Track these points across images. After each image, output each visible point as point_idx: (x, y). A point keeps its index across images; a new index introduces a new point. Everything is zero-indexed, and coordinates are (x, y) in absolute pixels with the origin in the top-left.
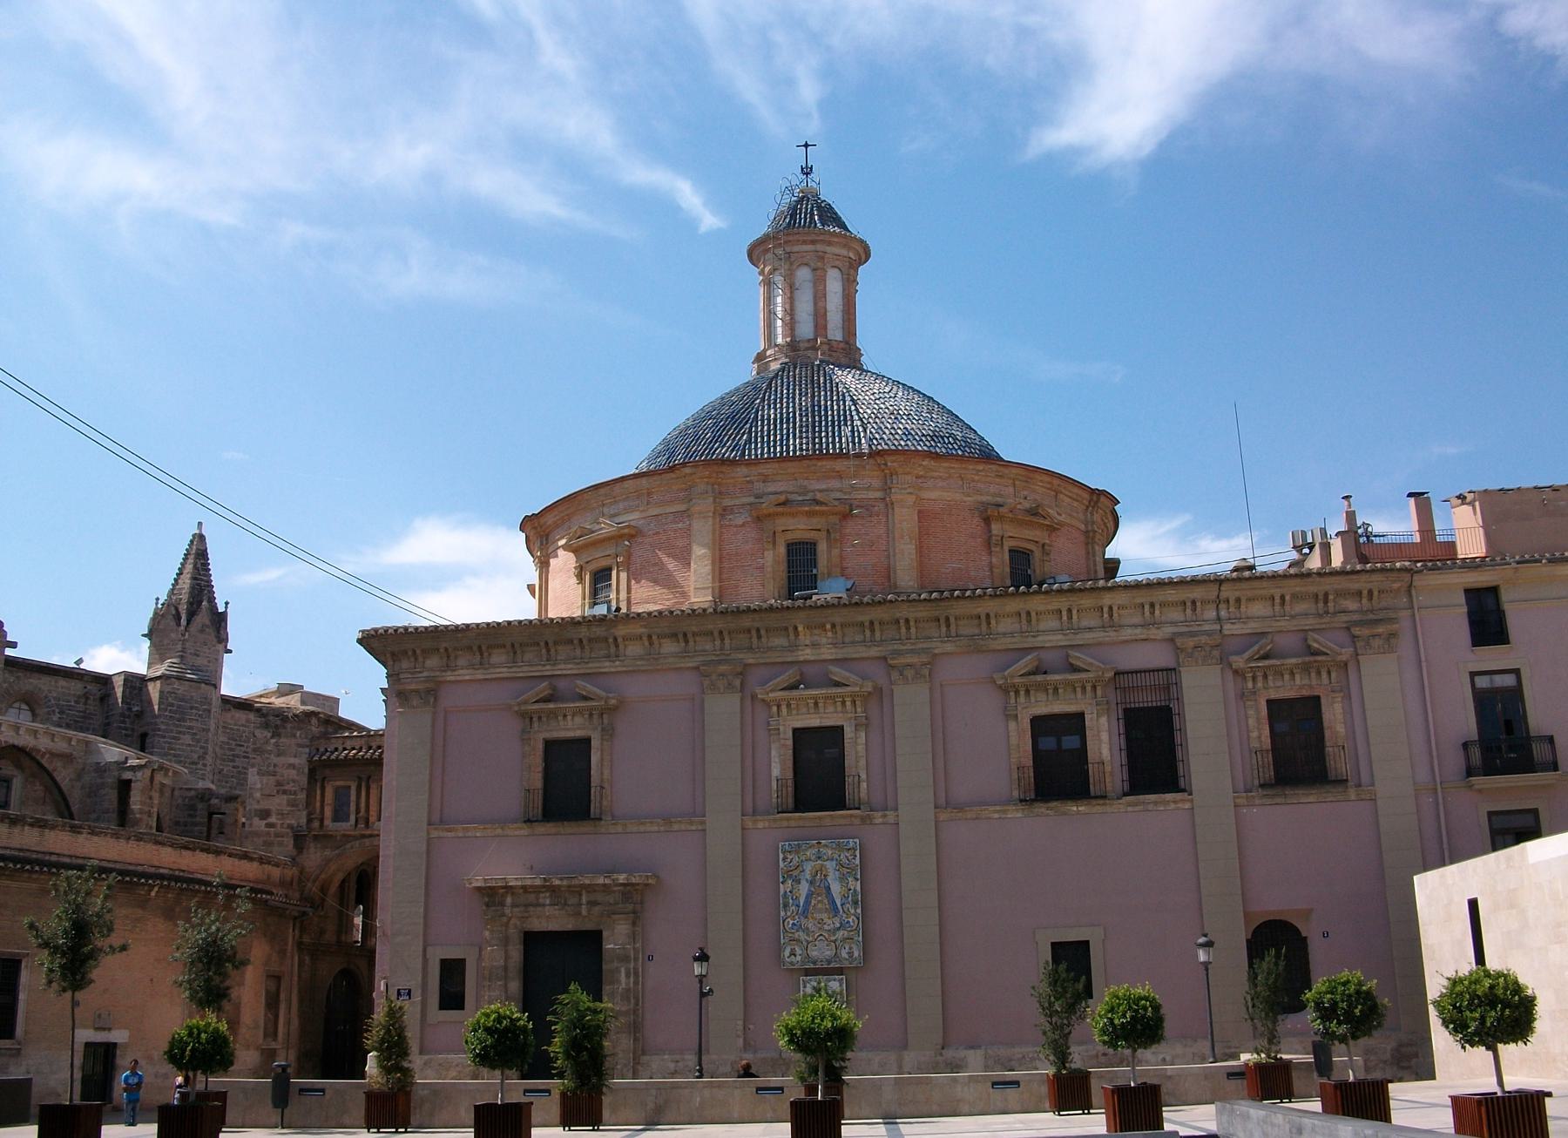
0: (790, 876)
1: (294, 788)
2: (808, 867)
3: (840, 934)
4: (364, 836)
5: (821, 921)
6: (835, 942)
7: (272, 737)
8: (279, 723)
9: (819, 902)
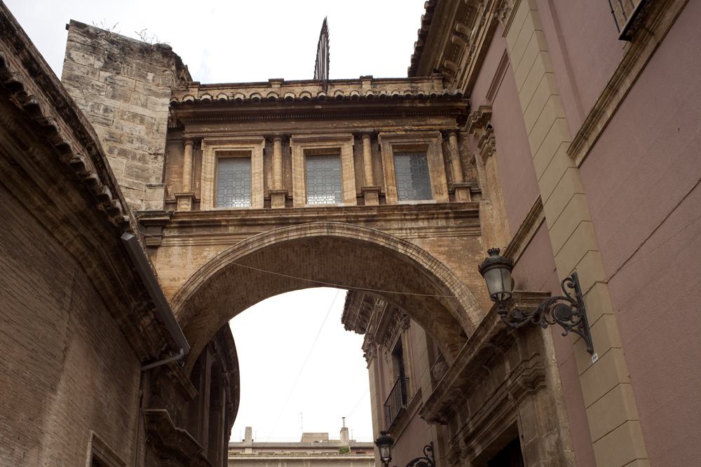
1: (140, 152)
4: (283, 222)
7: (105, 68)
8: (116, 51)
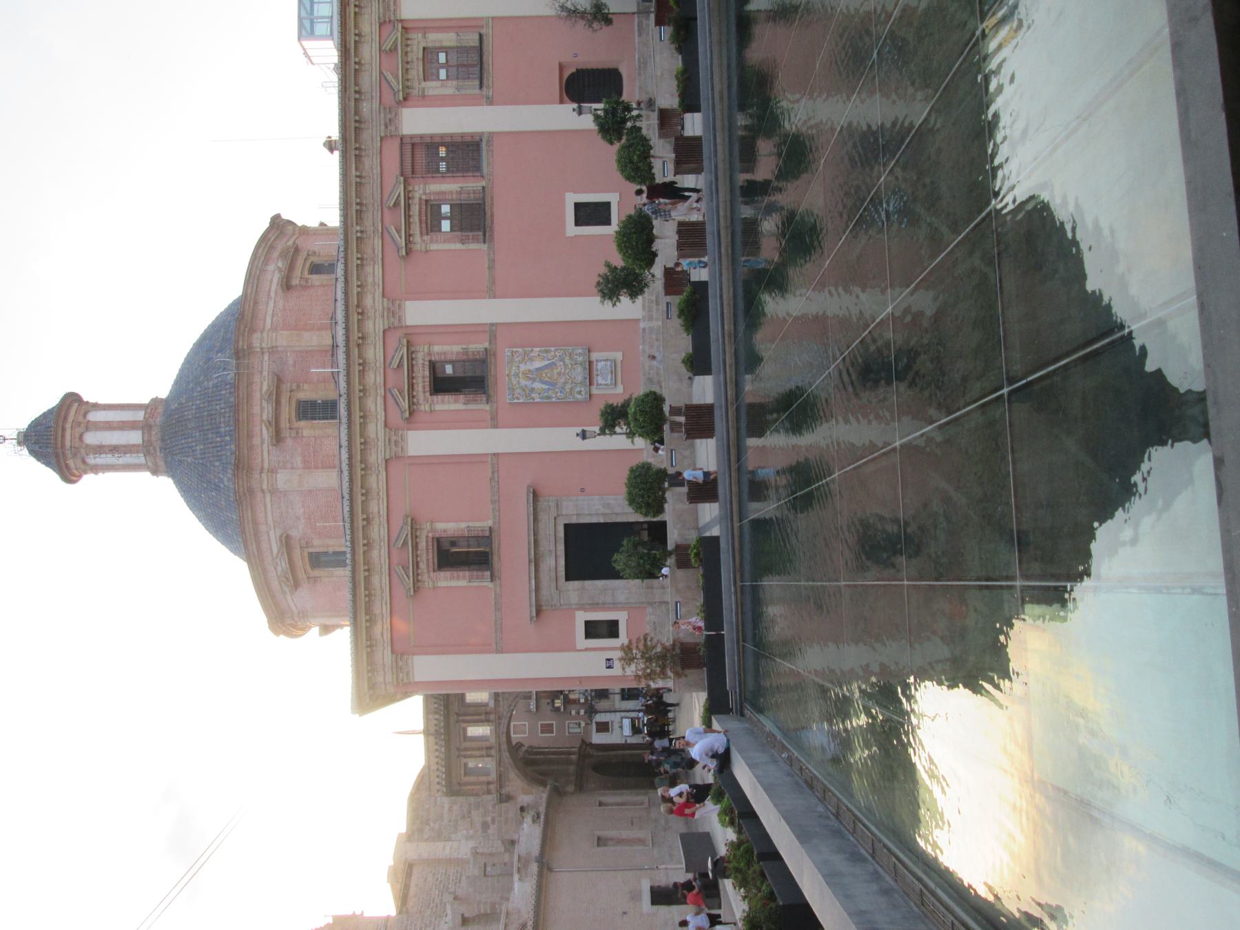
0: (529, 395)
2: (524, 382)
3: (567, 361)
4: (500, 750)
5: (559, 374)
6: (572, 365)
7: (429, 825)
9: (546, 375)
